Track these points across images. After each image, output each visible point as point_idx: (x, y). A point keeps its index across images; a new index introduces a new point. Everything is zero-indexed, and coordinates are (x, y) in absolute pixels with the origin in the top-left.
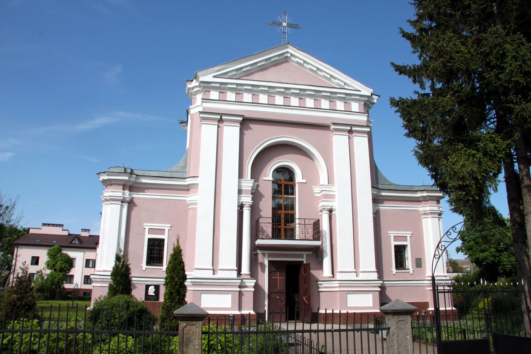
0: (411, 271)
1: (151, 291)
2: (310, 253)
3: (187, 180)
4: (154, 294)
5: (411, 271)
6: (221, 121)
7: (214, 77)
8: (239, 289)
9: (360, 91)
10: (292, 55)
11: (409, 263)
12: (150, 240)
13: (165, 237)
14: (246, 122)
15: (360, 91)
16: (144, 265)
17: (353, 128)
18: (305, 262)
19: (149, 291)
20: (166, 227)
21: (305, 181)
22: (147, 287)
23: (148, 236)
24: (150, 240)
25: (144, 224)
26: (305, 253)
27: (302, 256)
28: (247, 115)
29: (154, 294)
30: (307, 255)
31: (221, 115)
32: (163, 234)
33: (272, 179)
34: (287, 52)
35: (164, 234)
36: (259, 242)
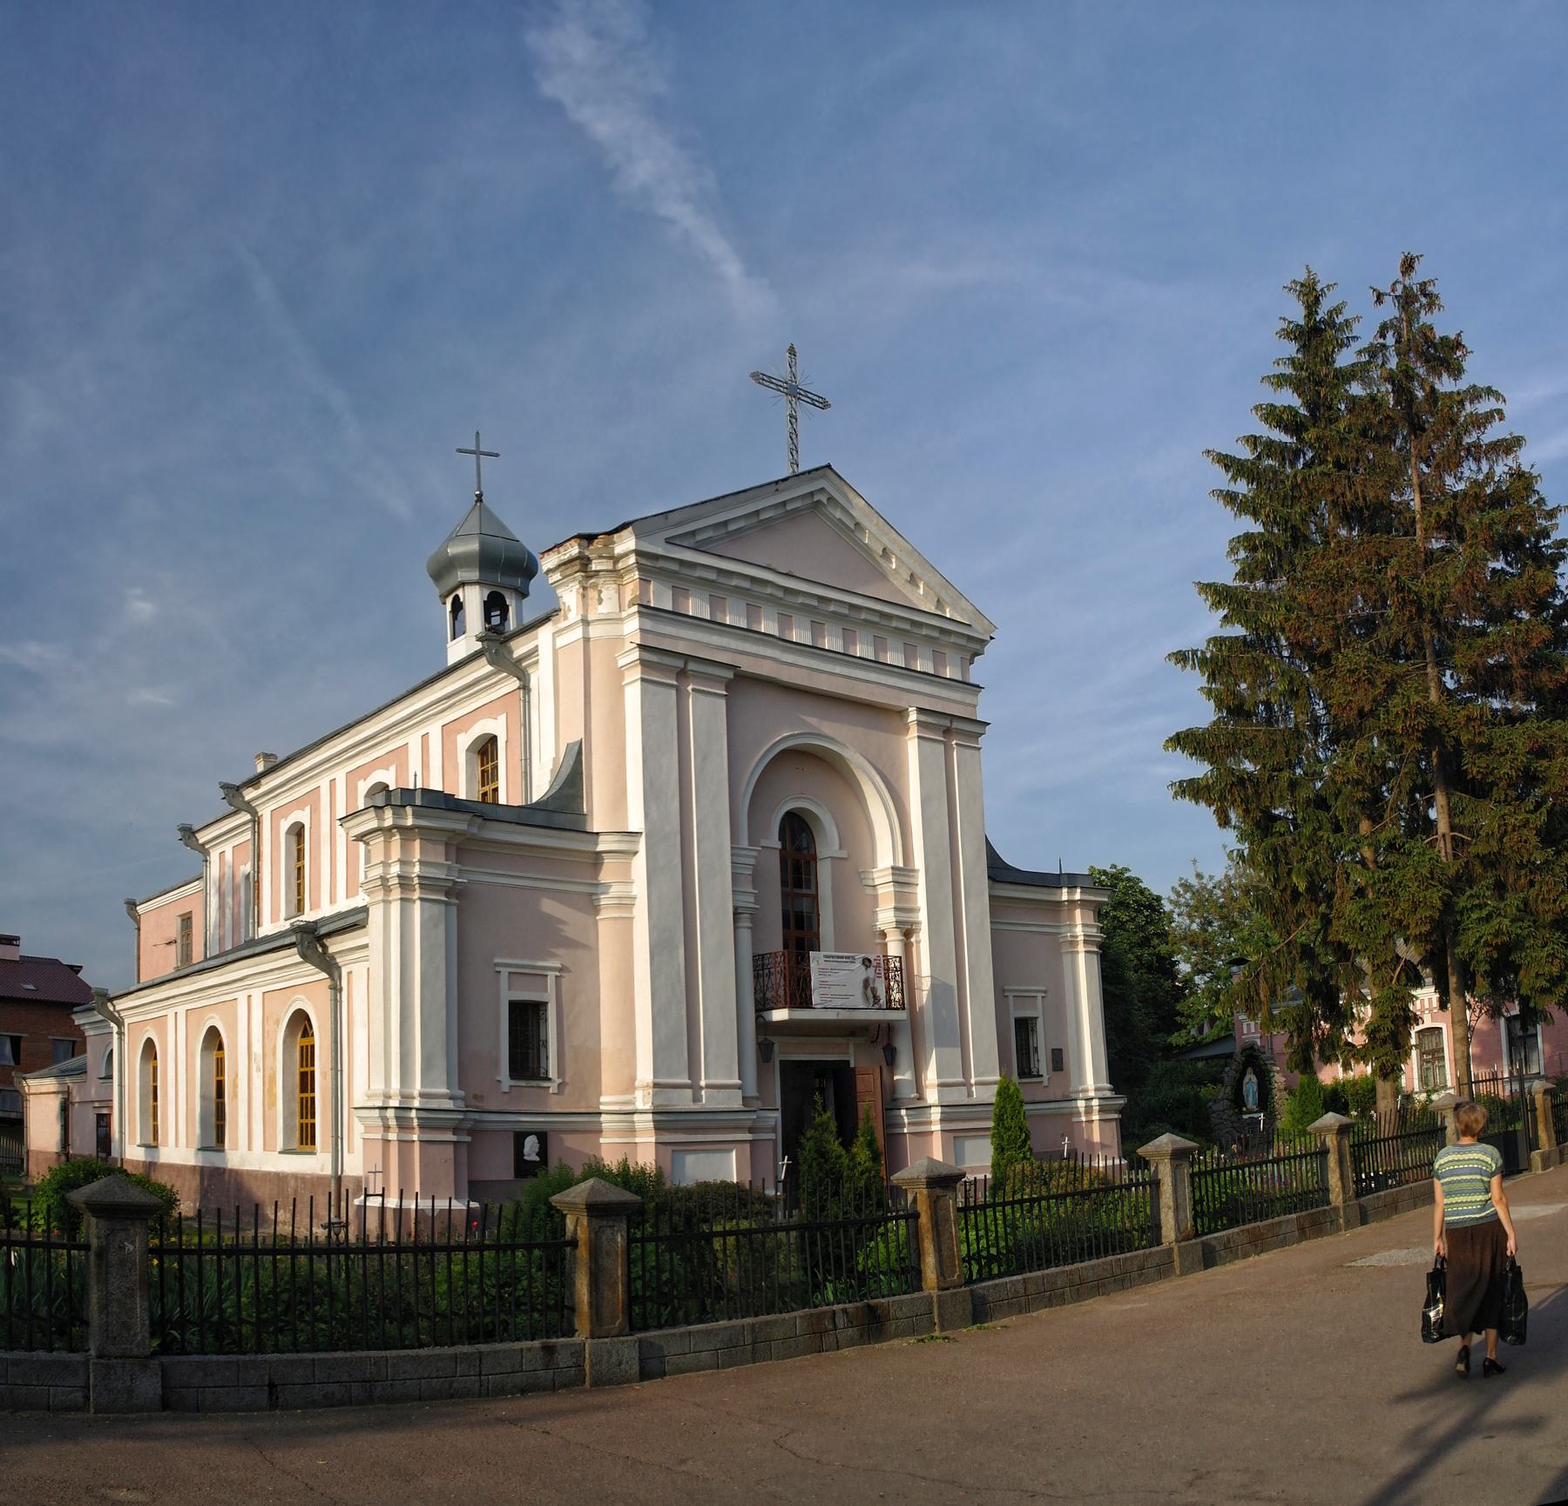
0: (1045, 1079)
1: (531, 1146)
3: (601, 838)
5: (1046, 1077)
6: (682, 674)
11: (1043, 1063)
14: (740, 683)
17: (956, 725)
19: (526, 1150)
21: (843, 854)
22: (520, 1137)
23: (508, 995)
25: (497, 960)
28: (747, 665)
31: (687, 658)
33: (778, 845)
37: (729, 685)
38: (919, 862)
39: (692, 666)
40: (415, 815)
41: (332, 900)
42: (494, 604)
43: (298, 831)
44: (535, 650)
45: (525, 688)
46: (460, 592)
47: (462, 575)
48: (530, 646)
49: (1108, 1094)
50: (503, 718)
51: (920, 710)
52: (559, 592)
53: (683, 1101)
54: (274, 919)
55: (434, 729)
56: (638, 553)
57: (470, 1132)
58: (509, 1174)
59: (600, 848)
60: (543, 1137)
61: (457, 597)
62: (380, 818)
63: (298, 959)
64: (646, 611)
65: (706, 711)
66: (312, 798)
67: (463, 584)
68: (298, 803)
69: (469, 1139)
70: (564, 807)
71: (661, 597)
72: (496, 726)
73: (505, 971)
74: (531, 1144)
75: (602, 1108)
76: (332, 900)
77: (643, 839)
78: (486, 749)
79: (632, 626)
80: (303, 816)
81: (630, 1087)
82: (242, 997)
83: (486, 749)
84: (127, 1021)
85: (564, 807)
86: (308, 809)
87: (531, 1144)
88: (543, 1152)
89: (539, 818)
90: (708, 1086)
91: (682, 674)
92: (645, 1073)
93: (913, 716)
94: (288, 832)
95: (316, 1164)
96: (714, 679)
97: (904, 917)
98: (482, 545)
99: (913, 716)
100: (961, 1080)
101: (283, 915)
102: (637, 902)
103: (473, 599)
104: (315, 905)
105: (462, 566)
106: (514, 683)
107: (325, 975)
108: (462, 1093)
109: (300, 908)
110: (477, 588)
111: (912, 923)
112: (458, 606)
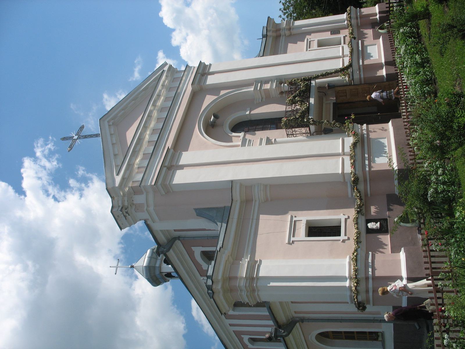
4: (379, 223)
7: (118, 175)
10: (112, 119)
16: (342, 237)
19: (374, 227)
22: (369, 231)
29: (379, 223)
34: (108, 122)
39: (166, 164)
44: (161, 231)
45: (179, 238)
48: (161, 233)
60: (368, 221)
61: (165, 275)
66: (238, 334)
67: (161, 273)
68: (241, 340)
72: (197, 251)
74: (371, 225)
80: (246, 338)
86: (242, 336)
87: (371, 225)
88: (376, 221)
94: (253, 344)
95: (388, 331)
106: (178, 243)
107: (298, 324)
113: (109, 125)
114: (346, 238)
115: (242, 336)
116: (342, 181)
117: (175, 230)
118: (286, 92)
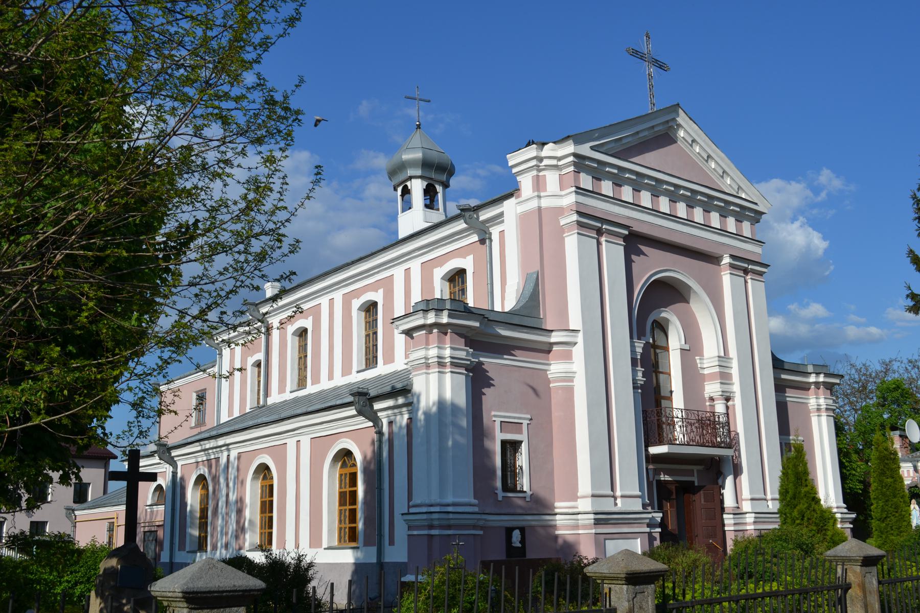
2: (700, 467)
3: (553, 334)
4: (520, 545)
6: (600, 232)
7: (592, 148)
8: (648, 530)
9: (756, 204)
12: (504, 443)
13: (523, 437)
15: (756, 204)
18: (696, 484)
20: (523, 418)
22: (509, 531)
24: (504, 443)
26: (695, 468)
27: (691, 473)
28: (637, 228)
29: (520, 545)
30: (698, 471)
32: (520, 432)
35: (520, 432)
36: (653, 450)
37: (625, 238)
38: (733, 352)
40: (450, 316)
41: (331, 377)
42: (430, 192)
43: (302, 333)
44: (501, 215)
46: (408, 184)
47: (410, 172)
49: (846, 511)
50: (470, 258)
51: (732, 257)
52: (519, 178)
53: (607, 505)
54: (282, 390)
55: (415, 266)
56: (575, 155)
57: (482, 528)
58: (503, 557)
59: (553, 340)
60: (522, 530)
61: (406, 186)
62: (425, 318)
63: (354, 412)
64: (580, 191)
65: (613, 253)
67: (410, 178)
69: (481, 532)
70: (528, 314)
71: (586, 181)
72: (467, 263)
73: (498, 420)
74: (516, 535)
75: (557, 511)
76: (331, 377)
77: (580, 335)
78: (457, 277)
79: (570, 199)
81: (575, 498)
82: (291, 443)
83: (457, 277)
84: (179, 464)
85: (528, 314)
87: (516, 535)
88: (523, 541)
89: (516, 321)
90: (622, 496)
91: (600, 232)
92: (585, 485)
93: (726, 260)
94: (294, 334)
96: (617, 235)
97: (726, 387)
98: (423, 154)
99: (726, 260)
100: (763, 496)
101: (288, 388)
102: (576, 375)
103: (417, 187)
104: (316, 381)
105: (410, 167)
107: (371, 424)
108: (476, 501)
109: (302, 384)
110: (419, 181)
111: (731, 392)
112: (406, 191)
113: (667, 122)
114: (500, 498)
115: (311, 318)
116: (579, 494)
117: (502, 232)
118: (713, 406)
